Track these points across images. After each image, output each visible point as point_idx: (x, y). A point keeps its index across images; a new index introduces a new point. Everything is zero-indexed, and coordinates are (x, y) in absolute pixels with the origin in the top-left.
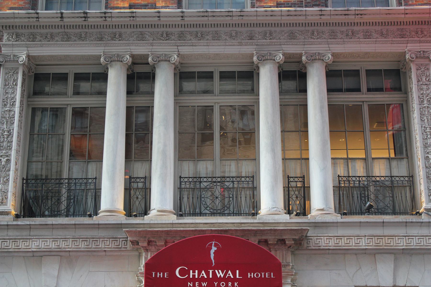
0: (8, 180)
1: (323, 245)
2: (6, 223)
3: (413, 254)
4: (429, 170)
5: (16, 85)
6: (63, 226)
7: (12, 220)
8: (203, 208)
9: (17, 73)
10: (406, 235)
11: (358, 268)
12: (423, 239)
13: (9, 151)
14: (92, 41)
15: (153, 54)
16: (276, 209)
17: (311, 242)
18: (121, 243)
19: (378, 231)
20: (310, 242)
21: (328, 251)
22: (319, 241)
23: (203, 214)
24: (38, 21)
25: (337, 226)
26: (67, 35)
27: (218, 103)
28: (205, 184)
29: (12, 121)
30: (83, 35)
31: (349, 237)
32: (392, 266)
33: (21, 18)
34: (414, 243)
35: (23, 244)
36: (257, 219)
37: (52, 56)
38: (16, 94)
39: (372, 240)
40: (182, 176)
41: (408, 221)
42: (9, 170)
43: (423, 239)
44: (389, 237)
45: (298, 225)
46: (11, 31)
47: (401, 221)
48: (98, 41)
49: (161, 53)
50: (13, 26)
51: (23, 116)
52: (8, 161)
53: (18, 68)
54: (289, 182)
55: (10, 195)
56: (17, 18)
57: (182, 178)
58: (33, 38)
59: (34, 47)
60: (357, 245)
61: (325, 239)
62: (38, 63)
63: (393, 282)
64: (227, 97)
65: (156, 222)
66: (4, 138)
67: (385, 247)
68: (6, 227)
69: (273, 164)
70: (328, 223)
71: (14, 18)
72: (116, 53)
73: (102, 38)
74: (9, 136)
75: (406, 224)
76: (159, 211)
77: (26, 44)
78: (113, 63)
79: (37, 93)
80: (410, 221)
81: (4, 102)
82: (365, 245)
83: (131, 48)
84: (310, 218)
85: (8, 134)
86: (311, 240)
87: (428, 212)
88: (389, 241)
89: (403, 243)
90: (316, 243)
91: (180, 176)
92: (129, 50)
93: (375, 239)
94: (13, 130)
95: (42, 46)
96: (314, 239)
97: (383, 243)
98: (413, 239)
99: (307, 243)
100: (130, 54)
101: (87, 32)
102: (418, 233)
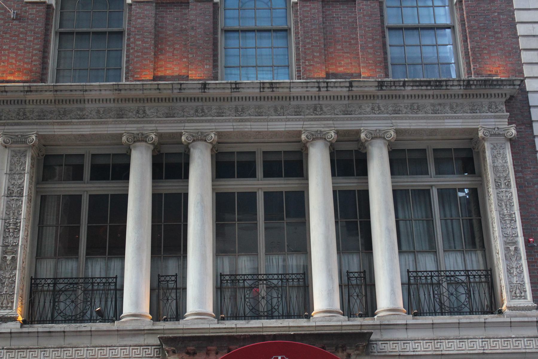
10: (37, 347)
28: (62, 286)
36: (181, 324)
54: (159, 282)
72: (20, 133)
98: (387, 343)
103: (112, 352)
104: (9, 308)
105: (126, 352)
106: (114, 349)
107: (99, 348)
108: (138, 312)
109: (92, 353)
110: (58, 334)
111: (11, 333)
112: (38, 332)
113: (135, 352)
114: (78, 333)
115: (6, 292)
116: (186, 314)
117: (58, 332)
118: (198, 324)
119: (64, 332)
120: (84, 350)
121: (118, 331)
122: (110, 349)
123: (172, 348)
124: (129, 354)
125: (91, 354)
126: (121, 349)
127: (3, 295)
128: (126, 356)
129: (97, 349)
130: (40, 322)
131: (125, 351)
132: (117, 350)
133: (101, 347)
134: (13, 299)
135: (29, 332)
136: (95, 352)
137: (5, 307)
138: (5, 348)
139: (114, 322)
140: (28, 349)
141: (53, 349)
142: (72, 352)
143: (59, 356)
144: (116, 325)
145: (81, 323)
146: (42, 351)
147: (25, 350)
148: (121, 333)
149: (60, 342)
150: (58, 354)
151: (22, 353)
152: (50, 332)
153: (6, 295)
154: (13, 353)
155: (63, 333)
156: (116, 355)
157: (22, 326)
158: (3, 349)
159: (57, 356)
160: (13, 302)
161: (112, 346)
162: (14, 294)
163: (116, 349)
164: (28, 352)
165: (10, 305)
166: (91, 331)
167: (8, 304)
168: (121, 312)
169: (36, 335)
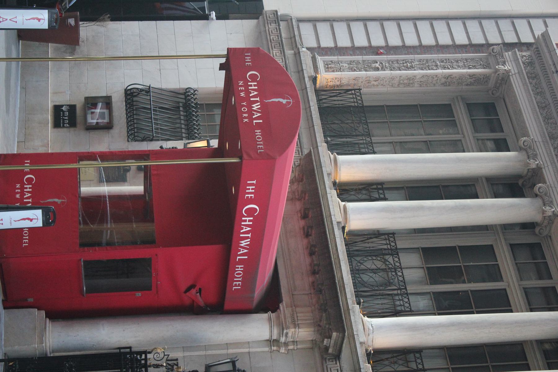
0: (355, 70)
2: (304, 68)
5: (470, 68)
6: (310, 118)
7: (310, 75)
8: (358, 259)
9: (484, 68)
13: (389, 70)
14: (547, 130)
15: (548, 187)
17: (332, 363)
20: (332, 361)
23: (351, 259)
24: (553, 73)
26: (546, 106)
27: (509, 286)
29: (425, 69)
30: (550, 121)
33: (552, 58)
35: (279, 59)
37: (516, 101)
38: (458, 69)
40: (395, 236)
42: (366, 71)
45: (346, 308)
46: (534, 57)
48: (549, 135)
49: (553, 196)
50: (553, 90)
51: (436, 88)
52: (377, 69)
53: (490, 68)
55: (338, 74)
56: (550, 54)
57: (394, 235)
58: (533, 76)
59: (521, 79)
62: (507, 100)
64: (521, 300)
65: (329, 199)
66: (403, 63)
68: (300, 69)
69: (433, 325)
71: (550, 52)
73: (553, 139)
74: (407, 67)
76: (345, 206)
77: (522, 71)
78: (524, 153)
79: (471, 107)
81: (446, 60)
83: (550, 167)
85: (409, 66)
91: (395, 234)
92: (546, 165)
94: (415, 70)
95: (524, 84)
100: (541, 164)
101: (556, 124)
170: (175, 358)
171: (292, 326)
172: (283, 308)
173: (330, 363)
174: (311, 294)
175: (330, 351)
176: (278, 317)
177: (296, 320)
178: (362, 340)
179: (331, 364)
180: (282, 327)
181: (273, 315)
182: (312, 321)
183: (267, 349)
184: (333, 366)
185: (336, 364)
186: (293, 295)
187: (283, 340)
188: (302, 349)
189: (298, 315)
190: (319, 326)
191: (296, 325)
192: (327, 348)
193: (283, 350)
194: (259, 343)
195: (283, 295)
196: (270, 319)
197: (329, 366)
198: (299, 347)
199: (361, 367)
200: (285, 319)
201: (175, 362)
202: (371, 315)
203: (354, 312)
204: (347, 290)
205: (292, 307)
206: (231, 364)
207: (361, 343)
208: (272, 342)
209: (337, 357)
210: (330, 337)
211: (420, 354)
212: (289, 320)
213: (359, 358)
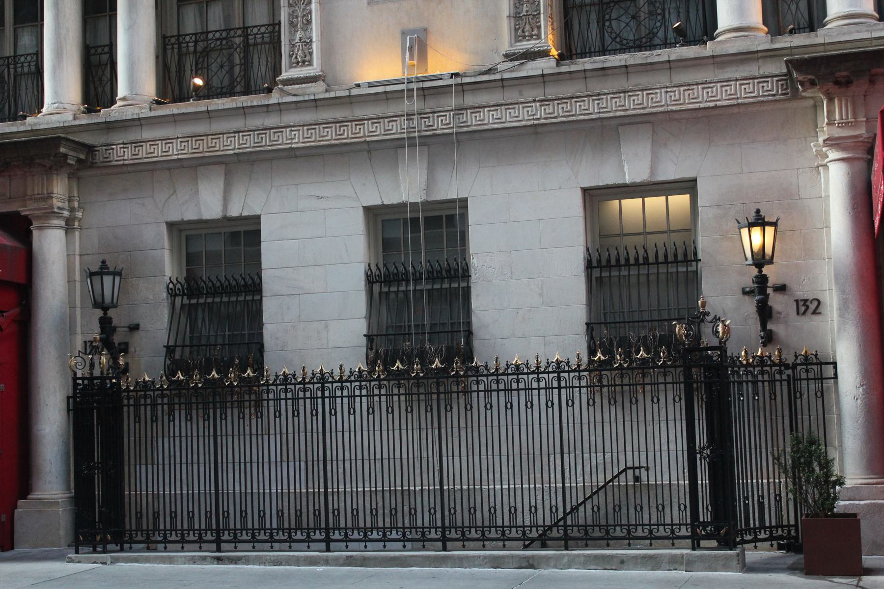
1: (116, 158)
3: (254, 161)
4: (294, 8)
10: (585, 93)
11: (171, 192)
12: (266, 133)
16: (57, 104)
17: (97, 155)
18: (435, 121)
19: (201, 128)
20: (96, 155)
21: (125, 169)
22: (110, 153)
25: (141, 125)
31: (168, 140)
32: (221, 183)
34: (249, 143)
36: (820, 37)
39: (188, 144)
41: (245, 105)
43: (266, 133)
44: (214, 137)
45: (28, 134)
47: (235, 106)
60: (306, 140)
61: (119, 149)
63: (223, 212)
67: (207, 154)
70: (123, 120)
75: (244, 111)
80: (249, 104)
82: (177, 153)
84: (115, 112)
86: (97, 153)
87: (284, 86)
88: (213, 143)
89: (235, 144)
90: (105, 156)
93: (193, 143)
96: (102, 149)
97: (203, 148)
99: (92, 156)
102: (263, 125)
103: (708, 92)
104: (535, 37)
105: (731, 90)
106: (710, 87)
107: (686, 88)
108: (744, 24)
109: (675, 96)
110: (617, 71)
111: (543, 75)
112: (585, 71)
113: (745, 89)
114: (649, 67)
115: (527, 12)
116: (827, 19)
117: (616, 67)
118: (850, 33)
119: (626, 66)
120: (661, 93)
121: (713, 57)
122: (703, 88)
123: (810, 77)
124: (736, 93)
125: (673, 98)
126: (722, 86)
127: (523, 17)
128: (731, 97)
129: (682, 89)
130: (583, 55)
131: (728, 88)
132: (714, 89)
133: (689, 85)
134: (540, 22)
135: (570, 72)
136: (680, 95)
137: (528, 36)
138: (537, 99)
139: (705, 43)
140: (572, 98)
141: (612, 96)
142: (643, 97)
143: (623, 106)
144: (710, 49)
145: (650, 50)
146: (595, 100)
147: (568, 101)
148: (719, 59)
149: (621, 83)
150: (620, 102)
151: (564, 105)
152: (603, 69)
153: (527, 17)
154: (551, 107)
155: (625, 69)
156: (714, 96)
157: (558, 64)
158: (534, 101)
159: (620, 106)
160: (539, 27)
161: (706, 83)
162: (539, 14)
163: (712, 87)
164: (573, 103)
165: (535, 32)
166: (669, 61)
167: (533, 31)
168: (715, 27)
169: (583, 74)
170: (83, 344)
171: (50, 202)
172: (26, 210)
173: (97, 158)
174: (10, 176)
175: (82, 157)
176: (38, 218)
177: (42, 196)
178: (71, 118)
179: (99, 157)
180: (52, 213)
181: (35, 224)
182: (45, 177)
183: (77, 233)
184: (101, 155)
185: (98, 151)
186: (10, 198)
187: (66, 213)
188: (78, 190)
189: (36, 192)
190: (50, 168)
191: (50, 196)
192: (79, 161)
193: (79, 214)
194: (69, 243)
195: (10, 210)
196: (40, 228)
197: (101, 160)
198: (76, 194)
199: (104, 120)
200: (40, 209)
201: (88, 344)
202: (40, 104)
203: (35, 124)
204: (8, 130)
205: (26, 200)
206: (93, 278)
207: (75, 118)
208: (69, 227)
209: (90, 149)
210: (65, 156)
211: (91, 48)
212: (42, 205)
213: (93, 122)
